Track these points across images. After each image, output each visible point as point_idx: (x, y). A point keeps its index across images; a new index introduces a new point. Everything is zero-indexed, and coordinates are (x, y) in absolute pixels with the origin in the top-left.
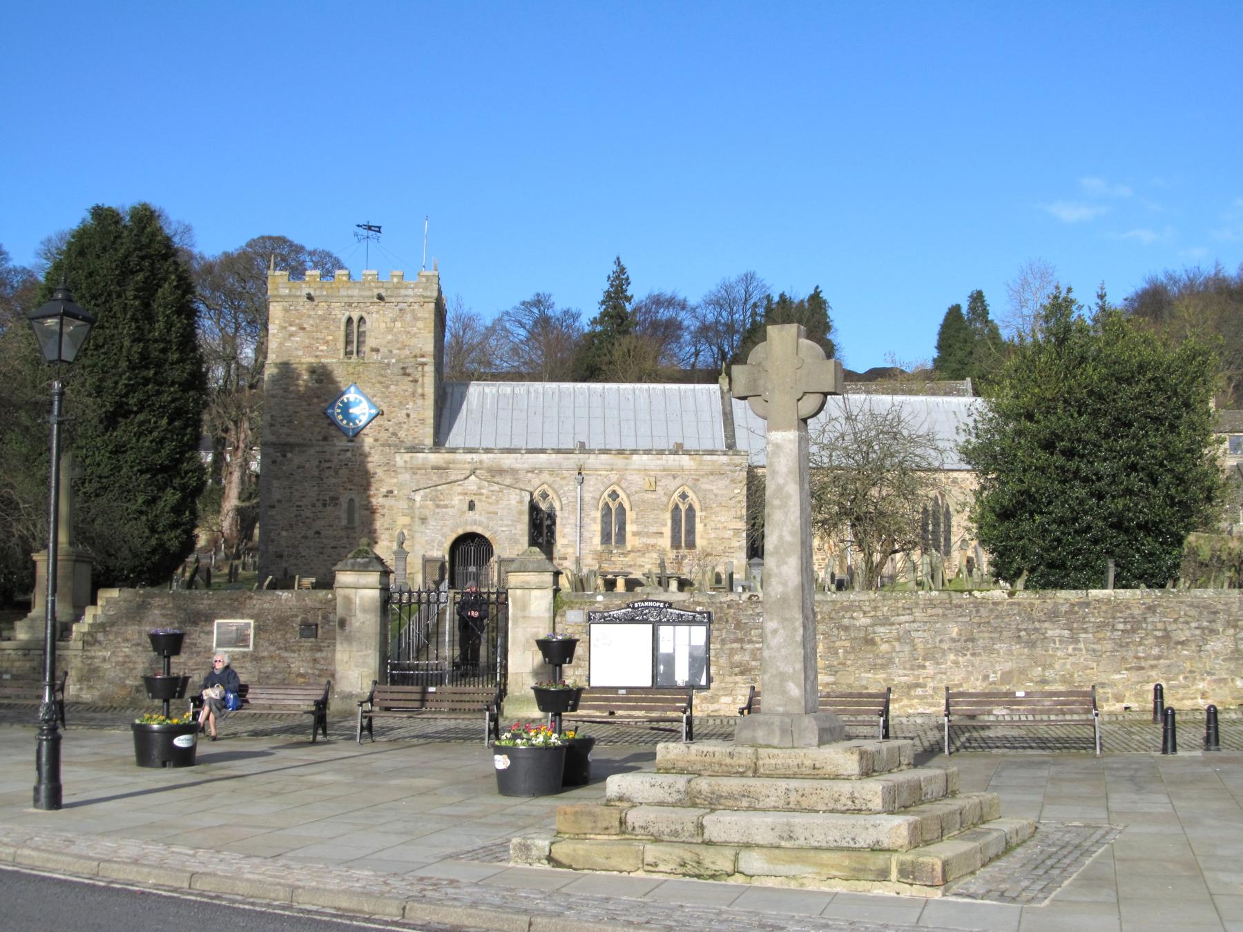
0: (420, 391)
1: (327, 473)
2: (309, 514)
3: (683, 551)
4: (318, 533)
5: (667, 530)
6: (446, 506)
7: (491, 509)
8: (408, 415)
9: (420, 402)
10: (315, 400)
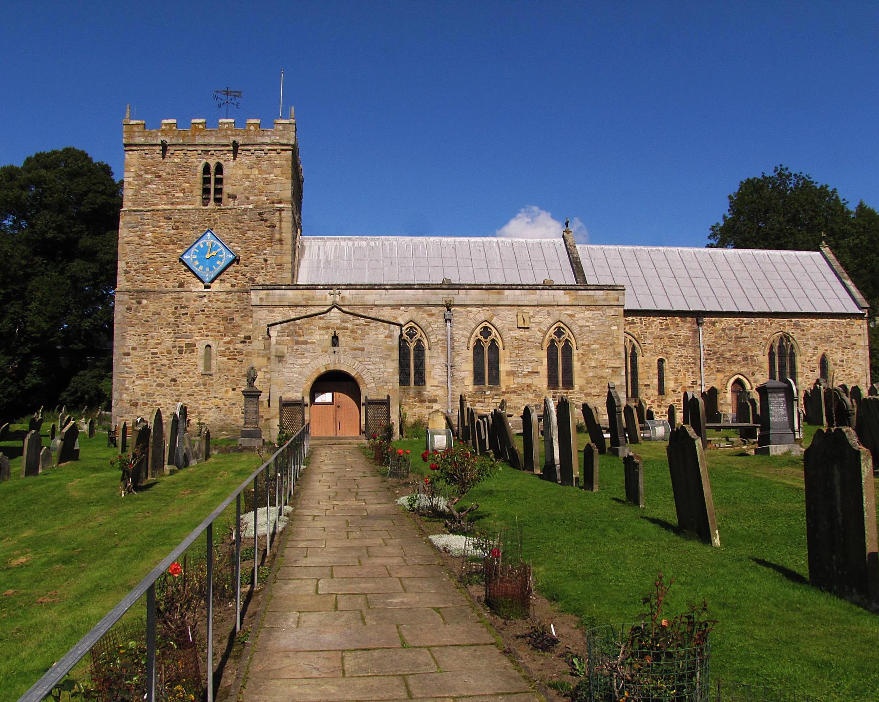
0: (277, 236)
1: (183, 319)
2: (165, 362)
4: (174, 380)
5: (543, 369)
6: (306, 343)
7: (358, 344)
8: (266, 260)
9: (278, 247)
10: (171, 247)
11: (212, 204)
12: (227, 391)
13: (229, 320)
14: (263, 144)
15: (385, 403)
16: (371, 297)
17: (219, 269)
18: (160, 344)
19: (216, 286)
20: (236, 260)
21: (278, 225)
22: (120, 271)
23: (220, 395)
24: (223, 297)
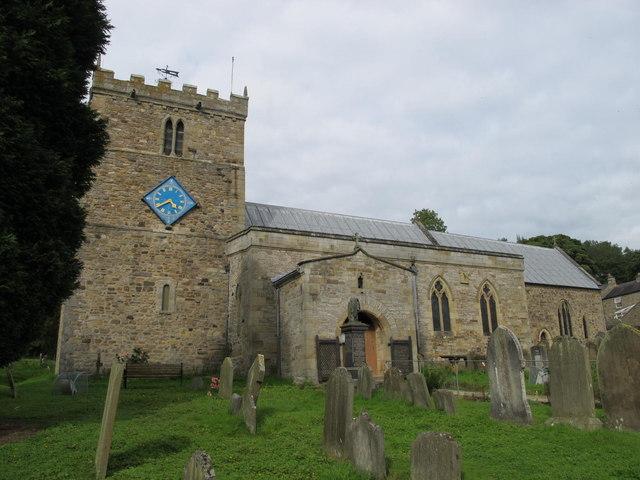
0: (233, 191)
4: (131, 318)
5: (479, 318)
6: (336, 282)
7: (380, 287)
9: (233, 200)
11: (173, 155)
12: (184, 332)
13: (188, 262)
14: (221, 111)
18: (118, 280)
19: (177, 229)
20: (196, 207)
21: (234, 180)
23: (177, 335)
24: (183, 239)
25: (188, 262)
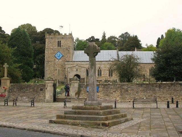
3: (111, 77)
5: (108, 74)
9: (69, 54)
11: (59, 47)
15: (84, 79)
16: (83, 63)
17: (60, 58)
19: (60, 60)
20: (63, 56)
22: (45, 58)
25: (62, 65)
